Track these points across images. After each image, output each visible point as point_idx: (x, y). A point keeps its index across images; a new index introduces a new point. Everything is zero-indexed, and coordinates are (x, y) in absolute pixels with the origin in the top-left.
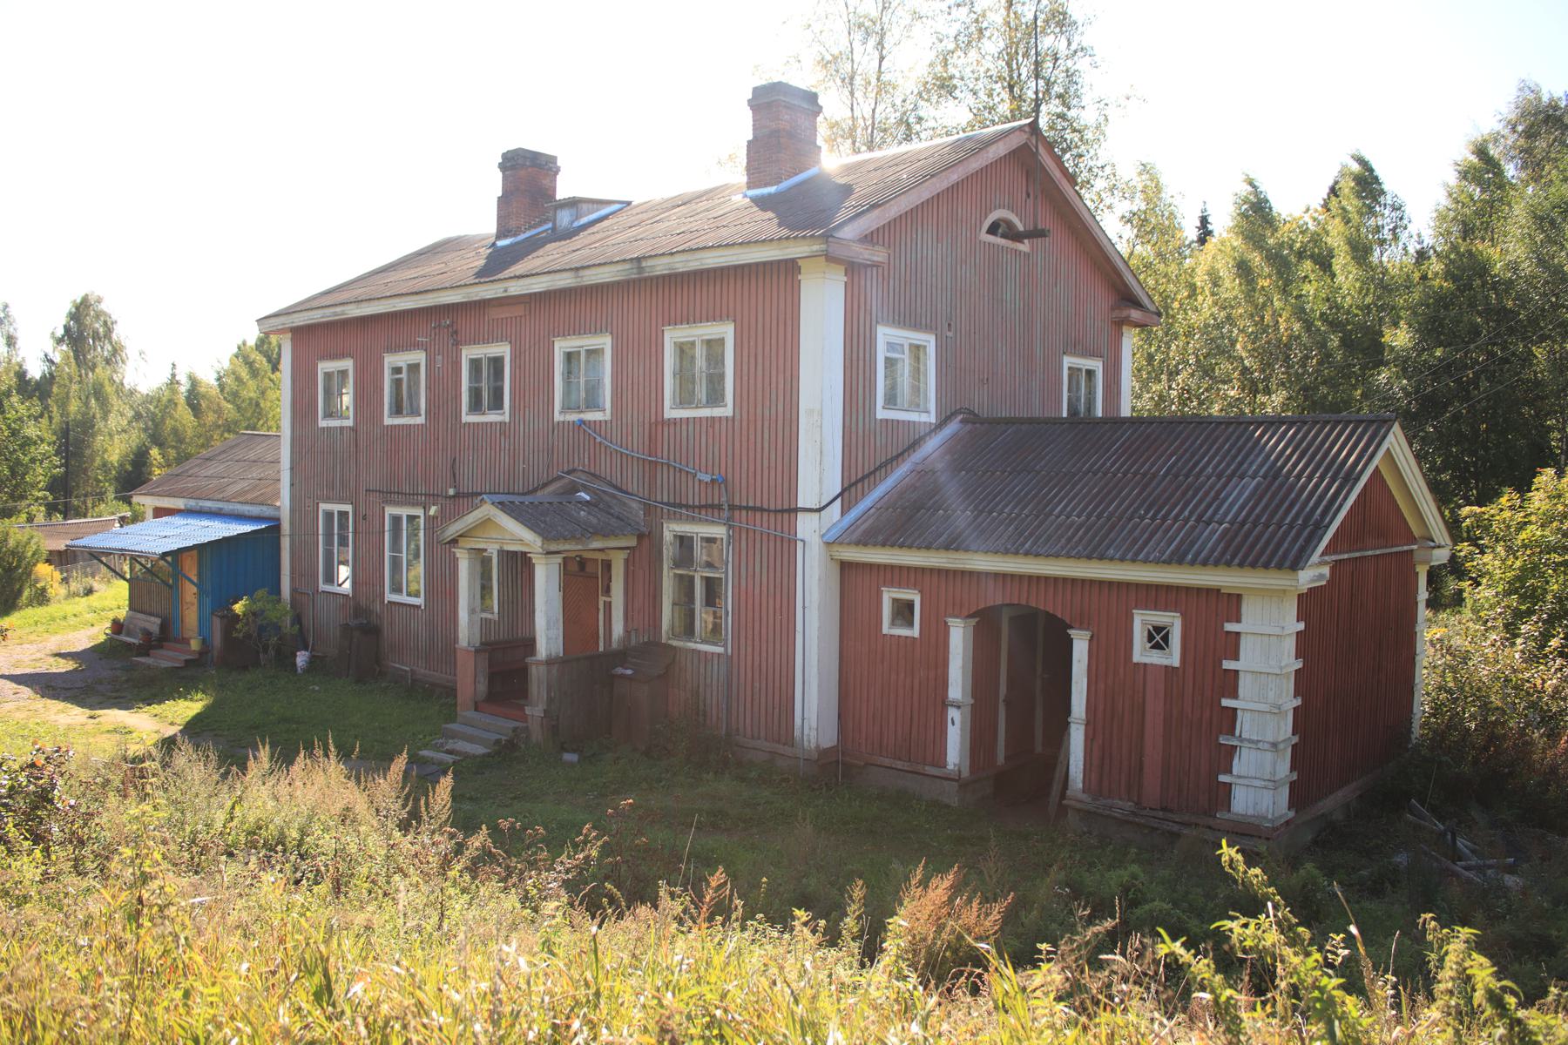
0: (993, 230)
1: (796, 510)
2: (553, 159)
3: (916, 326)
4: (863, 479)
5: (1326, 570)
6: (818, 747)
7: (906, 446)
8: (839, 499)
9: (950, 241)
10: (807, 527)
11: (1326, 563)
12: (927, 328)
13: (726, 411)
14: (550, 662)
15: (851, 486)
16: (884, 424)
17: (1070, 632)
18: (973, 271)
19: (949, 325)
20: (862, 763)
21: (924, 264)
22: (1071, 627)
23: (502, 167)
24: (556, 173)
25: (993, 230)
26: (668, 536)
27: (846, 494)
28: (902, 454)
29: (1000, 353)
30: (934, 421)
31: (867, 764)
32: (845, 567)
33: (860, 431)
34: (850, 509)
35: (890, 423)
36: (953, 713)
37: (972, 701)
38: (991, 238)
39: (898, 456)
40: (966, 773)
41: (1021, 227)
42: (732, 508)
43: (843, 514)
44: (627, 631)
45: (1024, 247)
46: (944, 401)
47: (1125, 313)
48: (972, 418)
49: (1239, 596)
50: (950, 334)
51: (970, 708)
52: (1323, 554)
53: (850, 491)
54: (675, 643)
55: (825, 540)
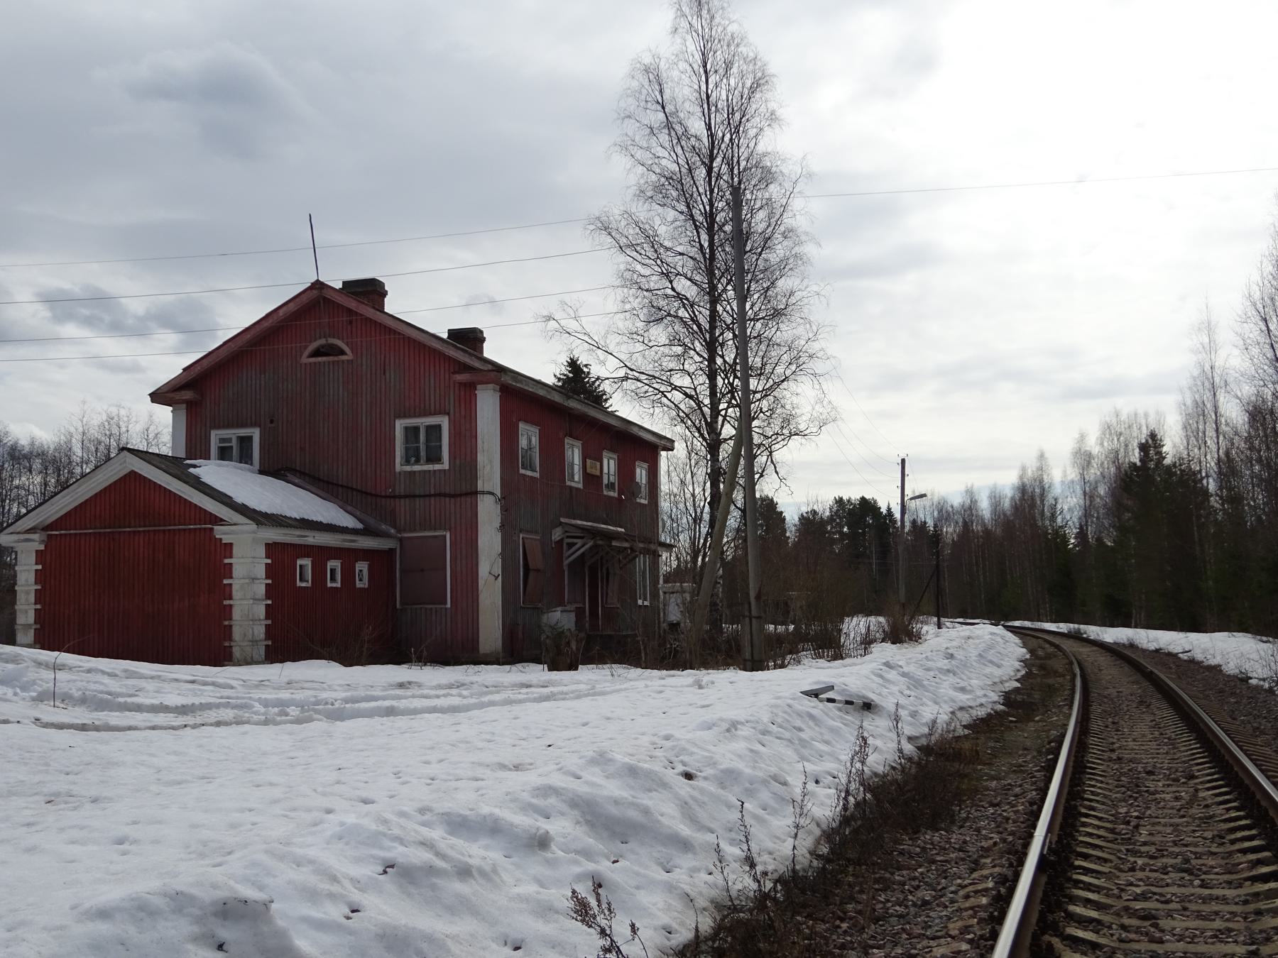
0: (317, 353)
12: (252, 425)
19: (272, 422)
25: (317, 353)
38: (312, 360)
50: (273, 425)
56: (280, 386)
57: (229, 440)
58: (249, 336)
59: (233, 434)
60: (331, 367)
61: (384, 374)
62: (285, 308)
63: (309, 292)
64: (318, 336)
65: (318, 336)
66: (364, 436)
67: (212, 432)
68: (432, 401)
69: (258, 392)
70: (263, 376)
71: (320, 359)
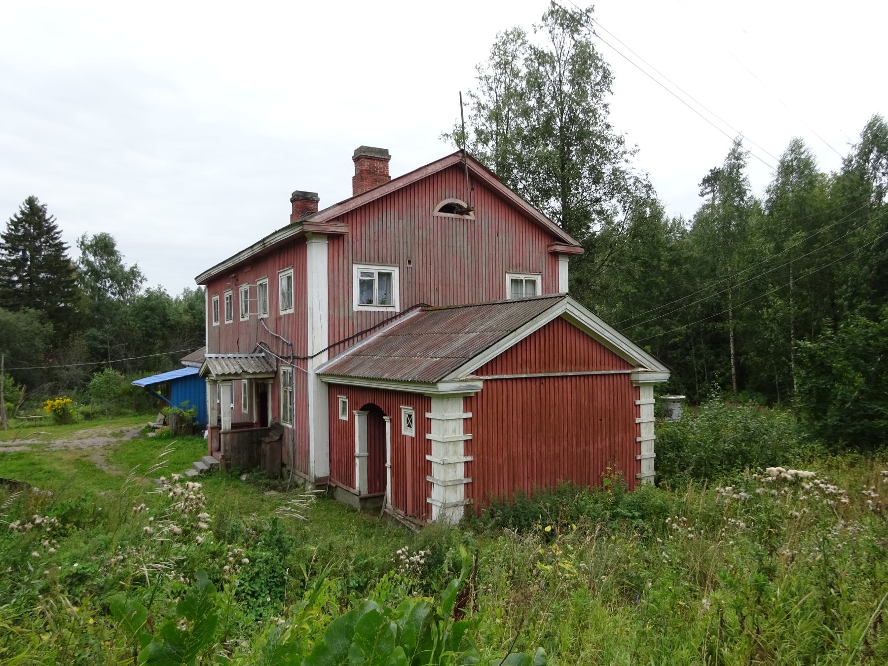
1: (306, 359)
2: (317, 194)
3: (383, 262)
4: (344, 341)
5: (480, 384)
6: (315, 476)
7: (377, 323)
8: (327, 352)
9: (409, 218)
10: (313, 367)
11: (480, 380)
12: (392, 264)
13: (291, 311)
14: (225, 433)
15: (334, 346)
16: (359, 314)
17: (384, 417)
18: (428, 232)
19: (410, 262)
20: (334, 485)
21: (389, 231)
22: (385, 415)
23: (292, 201)
24: (317, 201)
26: (282, 372)
27: (331, 349)
28: (375, 328)
29: (451, 274)
30: (397, 310)
31: (336, 487)
32: (330, 385)
33: (342, 318)
34: (334, 356)
35: (364, 314)
36: (357, 460)
37: (366, 454)
39: (370, 330)
40: (365, 492)
41: (465, 206)
42: (294, 358)
43: (329, 359)
44: (273, 418)
45: (471, 216)
46: (406, 301)
47: (554, 248)
48: (426, 307)
49: (430, 398)
50: (411, 266)
51: (366, 458)
52: (478, 372)
53: (333, 347)
54: (283, 424)
55: (317, 372)
56: (416, 232)
57: (371, 275)
58: (401, 184)
59: (375, 270)
60: (458, 223)
61: (498, 235)
62: (432, 167)
63: (452, 157)
64: (447, 195)
65: (447, 195)
66: (484, 283)
67: (354, 266)
68: (531, 262)
69: (397, 235)
70: (401, 221)
71: (449, 215)
